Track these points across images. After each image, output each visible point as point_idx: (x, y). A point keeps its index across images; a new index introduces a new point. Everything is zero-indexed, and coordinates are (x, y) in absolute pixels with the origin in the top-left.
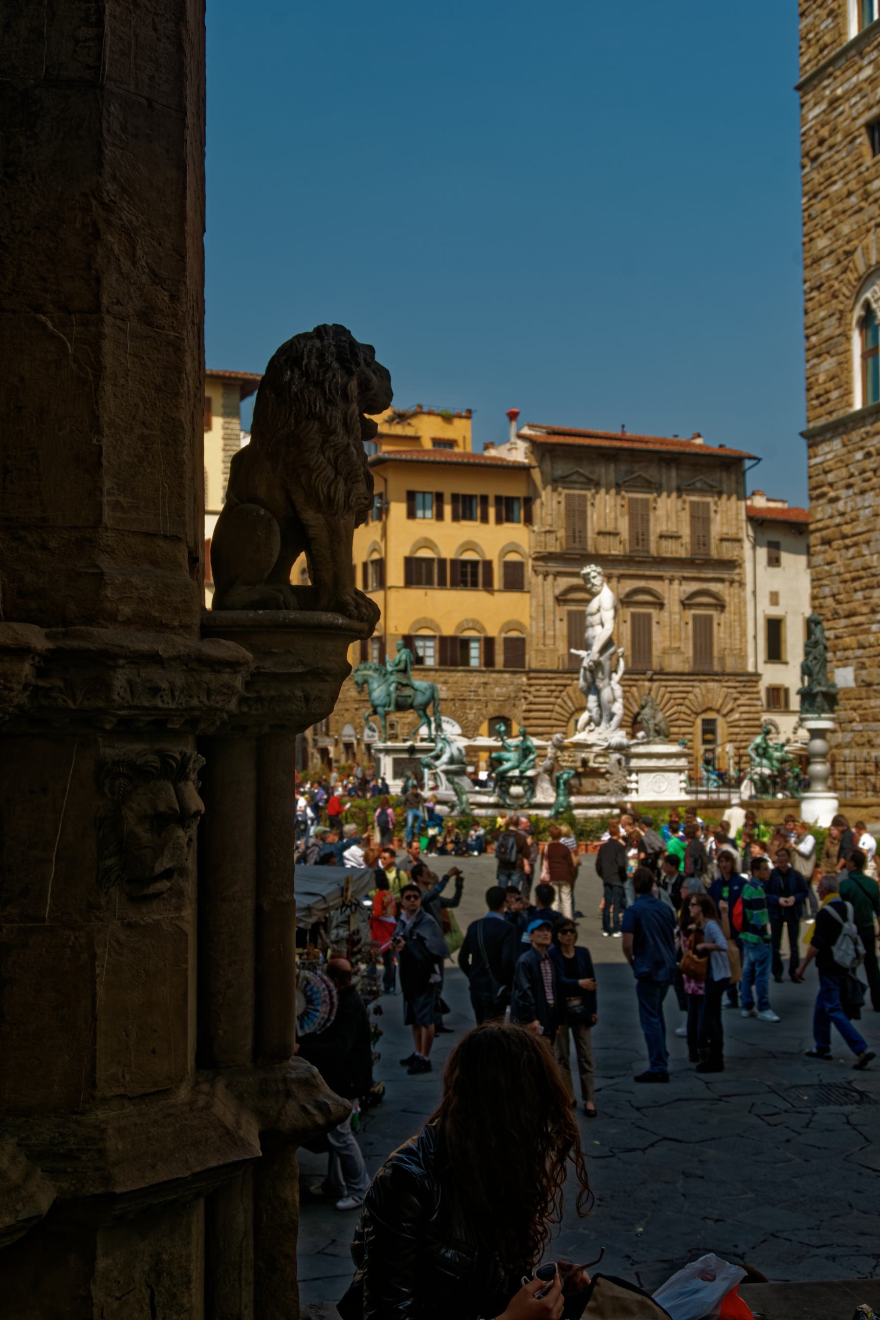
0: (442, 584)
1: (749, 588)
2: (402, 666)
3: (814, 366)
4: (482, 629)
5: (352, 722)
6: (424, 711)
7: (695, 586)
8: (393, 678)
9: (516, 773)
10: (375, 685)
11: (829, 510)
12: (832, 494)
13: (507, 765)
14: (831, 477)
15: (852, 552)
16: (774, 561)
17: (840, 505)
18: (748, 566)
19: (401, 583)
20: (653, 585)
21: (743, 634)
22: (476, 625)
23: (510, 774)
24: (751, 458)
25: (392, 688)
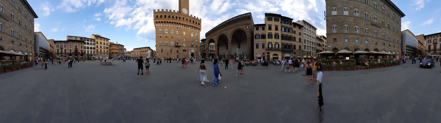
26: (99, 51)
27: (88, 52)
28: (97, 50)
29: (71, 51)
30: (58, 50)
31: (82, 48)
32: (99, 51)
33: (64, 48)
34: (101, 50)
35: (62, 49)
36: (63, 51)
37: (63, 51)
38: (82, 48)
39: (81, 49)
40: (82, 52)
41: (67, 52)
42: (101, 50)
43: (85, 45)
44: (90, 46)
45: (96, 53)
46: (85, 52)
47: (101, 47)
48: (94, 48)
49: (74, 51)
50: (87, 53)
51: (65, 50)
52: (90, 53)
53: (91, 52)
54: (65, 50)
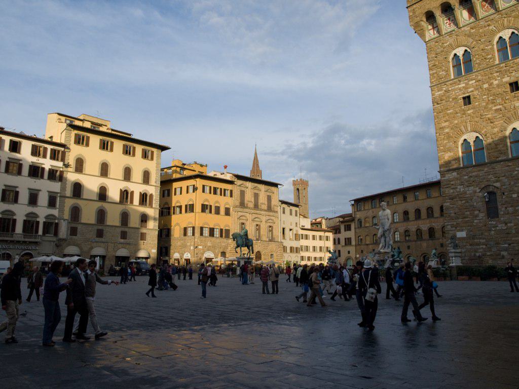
1: (280, 219)
3: (443, 154)
4: (220, 226)
5: (179, 252)
7: (268, 218)
9: (398, 259)
11: (452, 191)
12: (452, 187)
13: (396, 257)
14: (452, 183)
15: (464, 201)
16: (284, 212)
17: (458, 190)
18: (279, 214)
19: (200, 211)
20: (259, 216)
21: (278, 232)
22: (218, 225)
24: (280, 185)
25: (244, 240)
28: (76, 212)
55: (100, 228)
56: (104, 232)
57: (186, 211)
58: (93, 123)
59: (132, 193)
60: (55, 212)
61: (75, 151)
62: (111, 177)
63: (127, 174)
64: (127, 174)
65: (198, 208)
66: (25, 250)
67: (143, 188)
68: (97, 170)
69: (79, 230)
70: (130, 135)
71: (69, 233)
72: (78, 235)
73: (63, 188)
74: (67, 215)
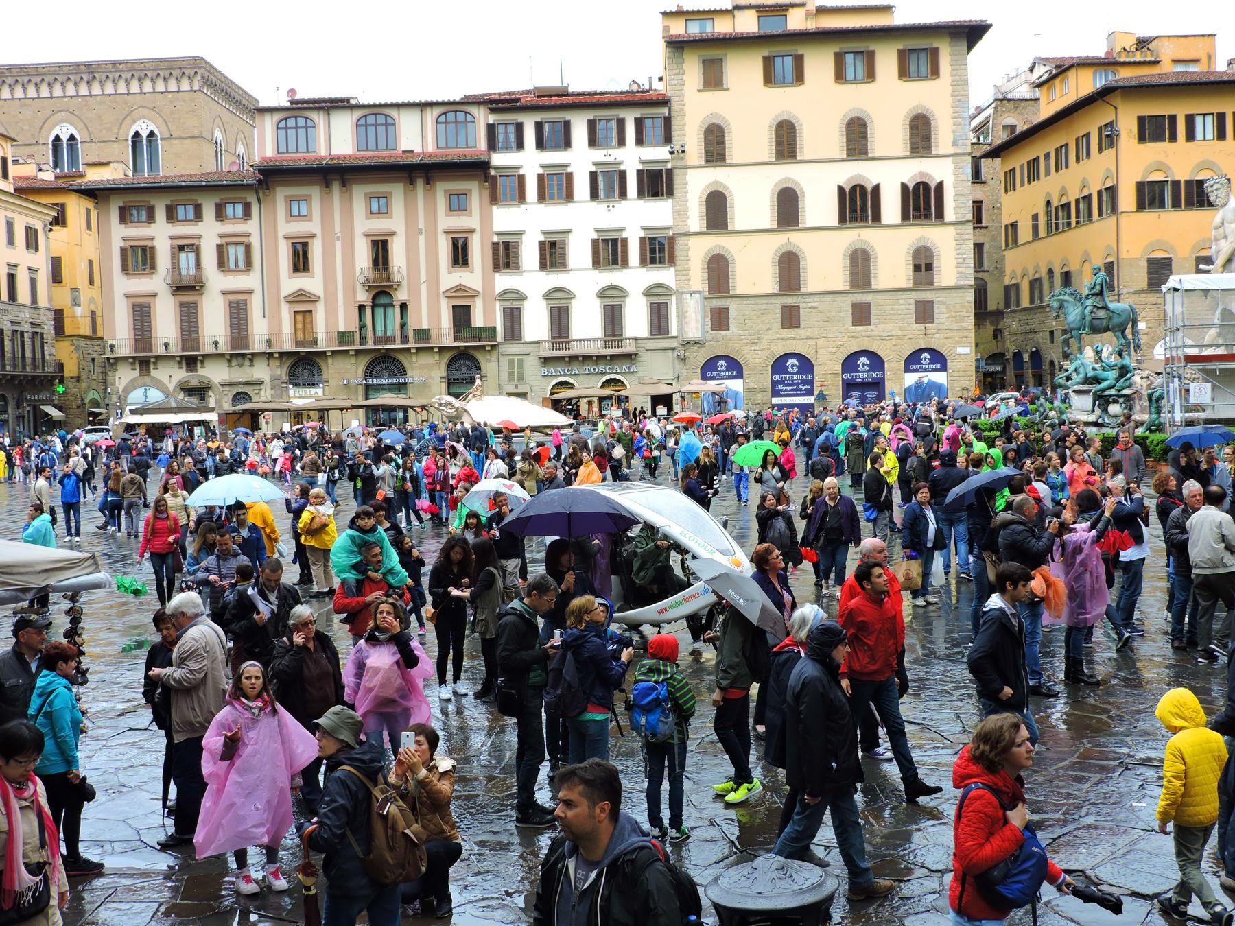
0: (1176, 204)
2: (1098, 289)
6: (1123, 332)
8: (1089, 302)
9: (1113, 392)
10: (1071, 309)
19: (1133, 207)
23: (1107, 393)
25: (1087, 312)
26: (754, 271)
27: (560, 319)
28: (719, 269)
29: (303, 315)
30: (142, 314)
31: (460, 254)
32: (754, 271)
33: (217, 282)
34: (789, 266)
35: (187, 289)
36: (214, 327)
37: (214, 327)
38: (460, 254)
39: (451, 278)
40: (462, 316)
41: (259, 331)
42: (789, 266)
43: (505, 218)
44: (583, 220)
45: (689, 318)
46: (513, 318)
47: (788, 206)
48: (658, 250)
49: (346, 321)
50: (536, 325)
51: (238, 311)
52: (587, 326)
53: (613, 316)
54: (238, 311)
55: (790, 301)
56: (802, 311)
57: (1100, 214)
58: (762, 10)
59: (877, 189)
60: (664, 275)
61: (695, 107)
62: (806, 157)
63: (857, 137)
64: (857, 137)
65: (1127, 199)
66: (605, 374)
67: (912, 170)
68: (765, 147)
69: (732, 315)
70: (886, 9)
71: (709, 323)
72: (732, 327)
73: (681, 214)
74: (698, 279)
